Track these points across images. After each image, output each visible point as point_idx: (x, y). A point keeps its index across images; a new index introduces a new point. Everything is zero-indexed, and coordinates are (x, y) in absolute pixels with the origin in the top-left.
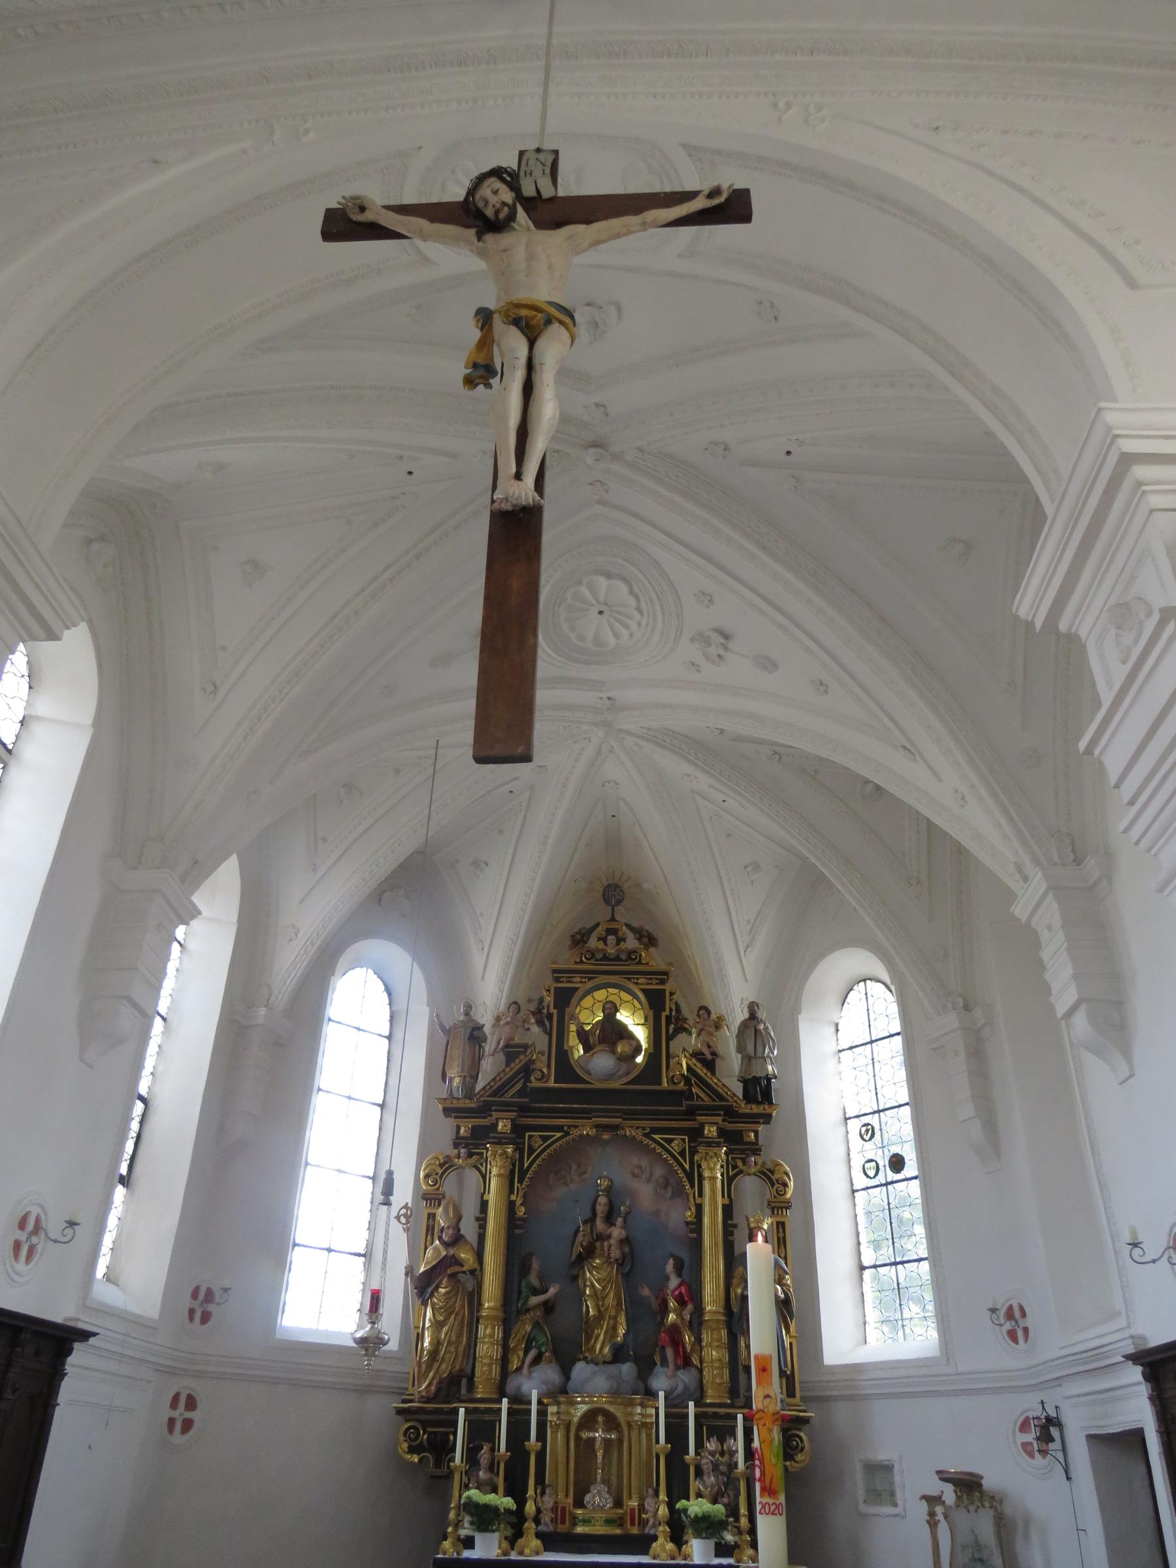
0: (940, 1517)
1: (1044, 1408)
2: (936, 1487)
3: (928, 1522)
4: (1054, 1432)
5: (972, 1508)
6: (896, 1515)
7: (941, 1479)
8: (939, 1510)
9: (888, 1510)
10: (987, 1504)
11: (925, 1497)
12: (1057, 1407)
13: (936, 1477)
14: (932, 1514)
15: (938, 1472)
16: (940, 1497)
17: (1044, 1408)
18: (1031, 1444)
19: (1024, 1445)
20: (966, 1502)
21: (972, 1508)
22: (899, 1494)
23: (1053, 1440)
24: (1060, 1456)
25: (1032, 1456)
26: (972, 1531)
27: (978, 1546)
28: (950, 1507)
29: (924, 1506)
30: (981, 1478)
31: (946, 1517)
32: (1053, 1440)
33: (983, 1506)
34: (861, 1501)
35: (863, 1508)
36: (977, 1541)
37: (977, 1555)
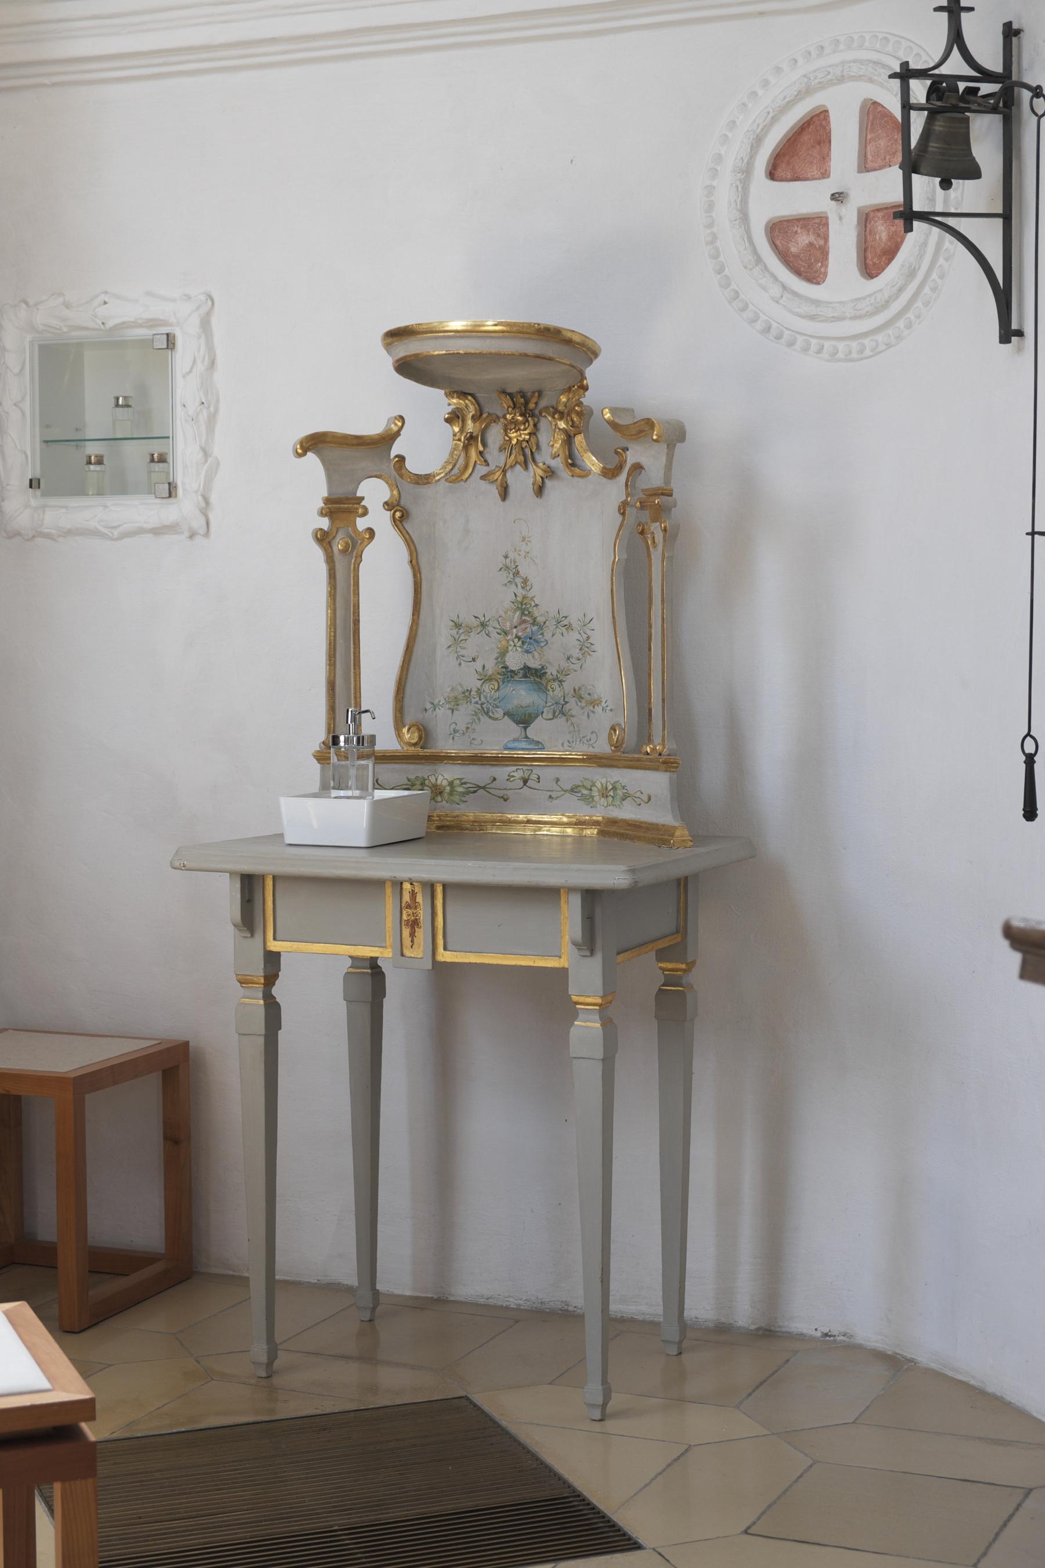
0: (377, 518)
1: (956, 38)
2: (371, 398)
3: (323, 538)
4: (984, 137)
5: (521, 480)
6: (171, 529)
7: (407, 368)
8: (374, 492)
9: (138, 510)
10: (592, 462)
11: (315, 443)
12: (1010, 33)
13: (386, 362)
14: (341, 507)
15: (396, 335)
16: (388, 439)
17: (956, 38)
18: (817, 224)
19: (779, 230)
20: (496, 458)
21: (521, 480)
22: (185, 452)
23: (973, 172)
24: (989, 238)
25: (809, 265)
26: (514, 572)
27: (528, 623)
28: (424, 480)
29: (312, 478)
30: (588, 352)
31: (400, 513)
32: (973, 172)
33: (573, 463)
34: (17, 481)
35: (22, 508)
36: (523, 607)
37: (515, 660)
